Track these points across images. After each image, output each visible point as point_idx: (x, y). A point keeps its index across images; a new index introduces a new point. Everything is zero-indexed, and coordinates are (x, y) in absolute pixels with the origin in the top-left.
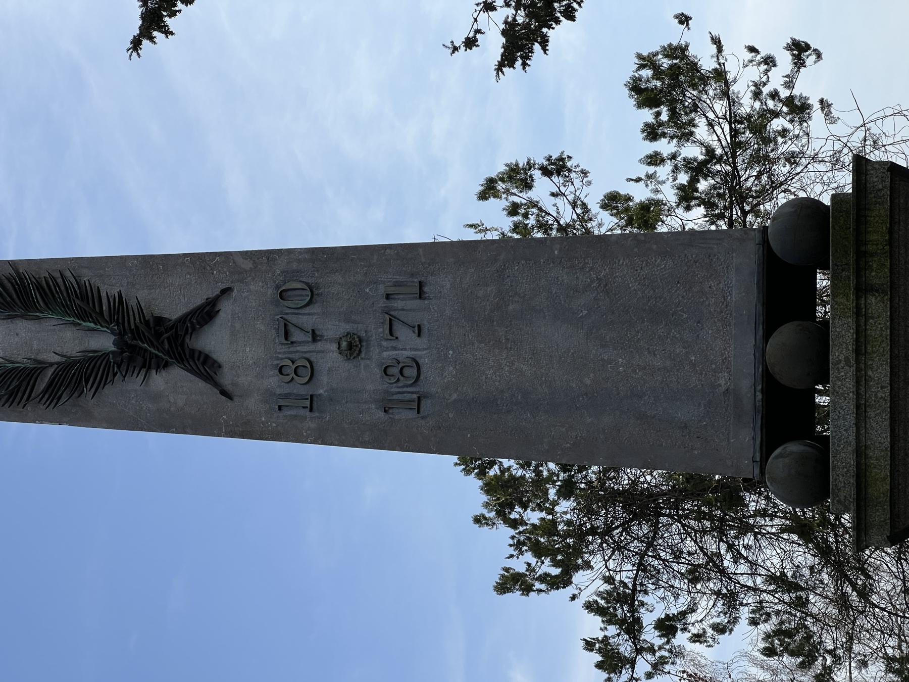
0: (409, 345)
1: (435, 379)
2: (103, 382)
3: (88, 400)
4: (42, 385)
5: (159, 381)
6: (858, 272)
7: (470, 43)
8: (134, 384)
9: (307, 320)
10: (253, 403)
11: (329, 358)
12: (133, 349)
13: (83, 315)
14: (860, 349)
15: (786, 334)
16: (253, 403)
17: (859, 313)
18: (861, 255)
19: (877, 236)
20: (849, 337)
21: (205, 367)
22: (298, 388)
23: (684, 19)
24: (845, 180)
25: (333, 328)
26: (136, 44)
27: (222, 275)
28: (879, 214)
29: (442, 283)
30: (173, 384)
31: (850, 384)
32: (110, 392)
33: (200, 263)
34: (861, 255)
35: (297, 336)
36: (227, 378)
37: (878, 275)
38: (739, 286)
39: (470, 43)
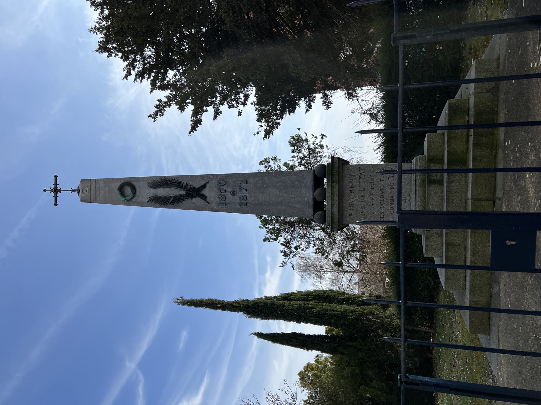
0: (244, 193)
1: (250, 199)
2: (183, 200)
3: (180, 204)
4: (171, 201)
5: (194, 200)
6: (332, 178)
7: (258, 133)
8: (189, 201)
9: (225, 188)
10: (214, 204)
11: (229, 195)
12: (189, 194)
13: (179, 187)
15: (318, 190)
16: (214, 204)
17: (332, 186)
19: (335, 171)
20: (330, 191)
21: (204, 197)
22: (222, 202)
23: (299, 129)
24: (329, 161)
25: (230, 190)
26: (190, 133)
27: (207, 179)
28: (336, 167)
29: (251, 181)
30: (197, 201)
31: (330, 200)
32: (184, 202)
33: (202, 177)
34: (332, 175)
35: (222, 191)
36: (208, 200)
37: (336, 179)
38: (309, 181)
39: (258, 133)
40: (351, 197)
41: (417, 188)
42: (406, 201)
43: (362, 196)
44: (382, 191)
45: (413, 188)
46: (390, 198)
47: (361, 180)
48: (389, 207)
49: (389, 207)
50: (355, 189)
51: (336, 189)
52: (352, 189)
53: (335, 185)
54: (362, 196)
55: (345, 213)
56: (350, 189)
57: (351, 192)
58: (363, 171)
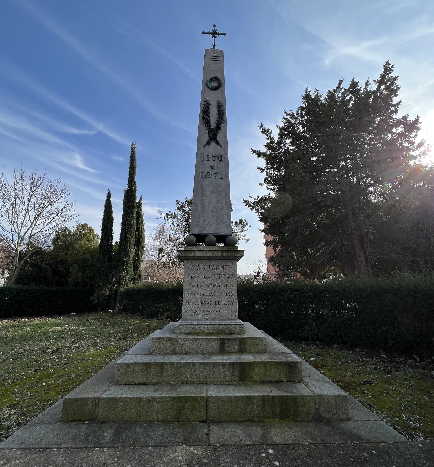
0: (212, 176)
1: (206, 180)
2: (206, 127)
3: (203, 124)
4: (206, 117)
5: (207, 135)
7: (250, 196)
8: (206, 131)
9: (217, 160)
10: (203, 151)
11: (210, 163)
12: (212, 131)
13: (217, 123)
14: (212, 251)
15: (214, 239)
16: (203, 151)
17: (218, 251)
18: (228, 251)
19: (231, 254)
20: (214, 249)
21: (209, 143)
22: (205, 158)
23: (251, 225)
25: (215, 164)
26: (252, 149)
27: (223, 146)
28: (235, 254)
29: (223, 182)
30: (206, 138)
31: (206, 249)
32: (205, 127)
33: (226, 143)
35: (214, 158)
36: (207, 146)
37: (224, 254)
38: (222, 231)
39: (250, 196)
40: (208, 267)
41: (216, 326)
42: (204, 315)
43: (209, 277)
44: (213, 294)
45: (216, 322)
46: (207, 302)
47: (223, 276)
48: (199, 300)
49: (199, 300)
50: (216, 271)
51: (216, 254)
52: (215, 268)
53: (219, 254)
54: (209, 277)
55: (195, 262)
56: (215, 266)
57: (213, 267)
58: (231, 277)
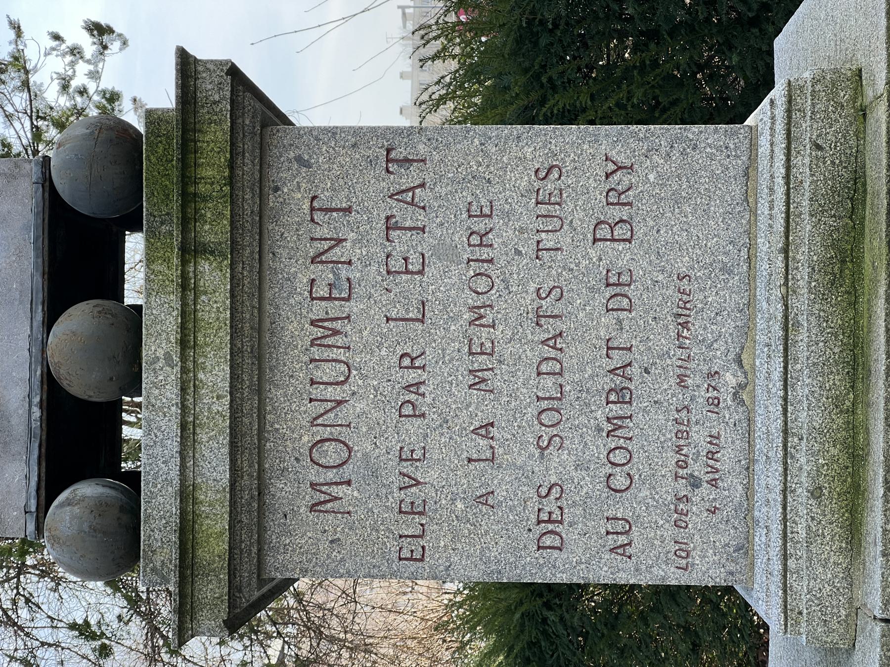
6: (184, 231)
14: (187, 341)
15: (79, 318)
17: (187, 286)
18: (189, 198)
19: (211, 170)
20: (171, 323)
24: (163, 95)
28: (214, 137)
31: (172, 393)
34: (189, 198)
37: (213, 229)
40: (327, 372)
41: (801, 303)
42: (714, 403)
43: (409, 361)
44: (551, 327)
45: (769, 307)
46: (607, 382)
47: (401, 242)
48: (598, 448)
49: (598, 448)
50: (354, 307)
51: (215, 307)
52: (334, 309)
53: (213, 275)
54: (409, 361)
55: (282, 489)
56: (318, 310)
57: (327, 330)
58: (408, 178)
